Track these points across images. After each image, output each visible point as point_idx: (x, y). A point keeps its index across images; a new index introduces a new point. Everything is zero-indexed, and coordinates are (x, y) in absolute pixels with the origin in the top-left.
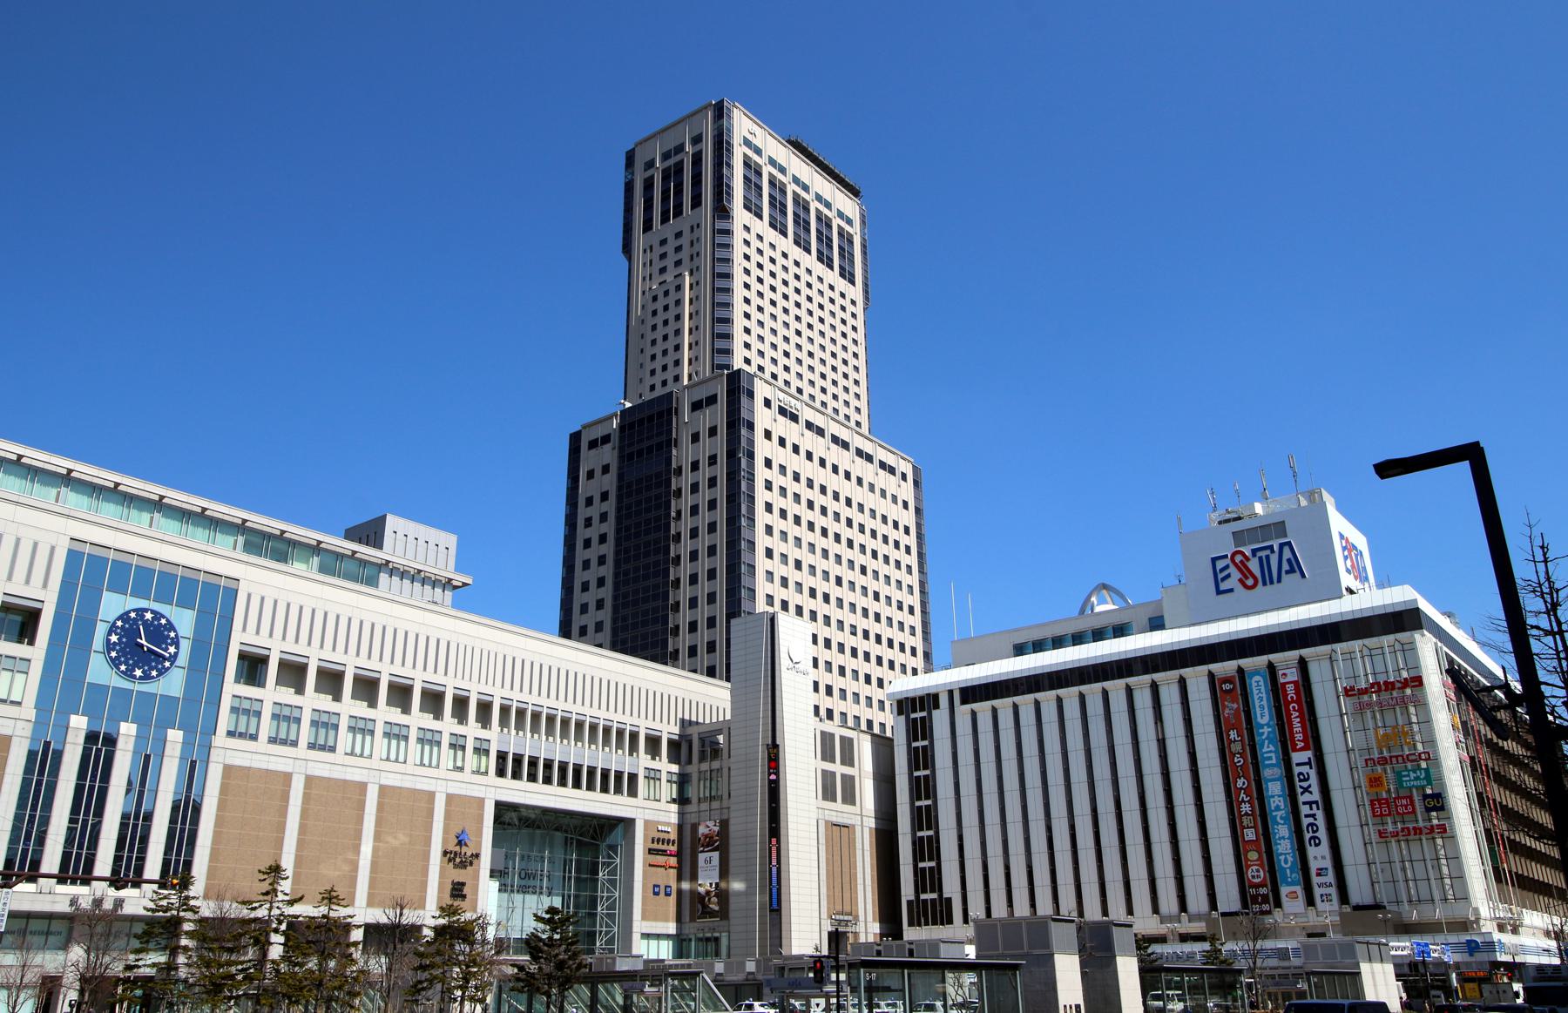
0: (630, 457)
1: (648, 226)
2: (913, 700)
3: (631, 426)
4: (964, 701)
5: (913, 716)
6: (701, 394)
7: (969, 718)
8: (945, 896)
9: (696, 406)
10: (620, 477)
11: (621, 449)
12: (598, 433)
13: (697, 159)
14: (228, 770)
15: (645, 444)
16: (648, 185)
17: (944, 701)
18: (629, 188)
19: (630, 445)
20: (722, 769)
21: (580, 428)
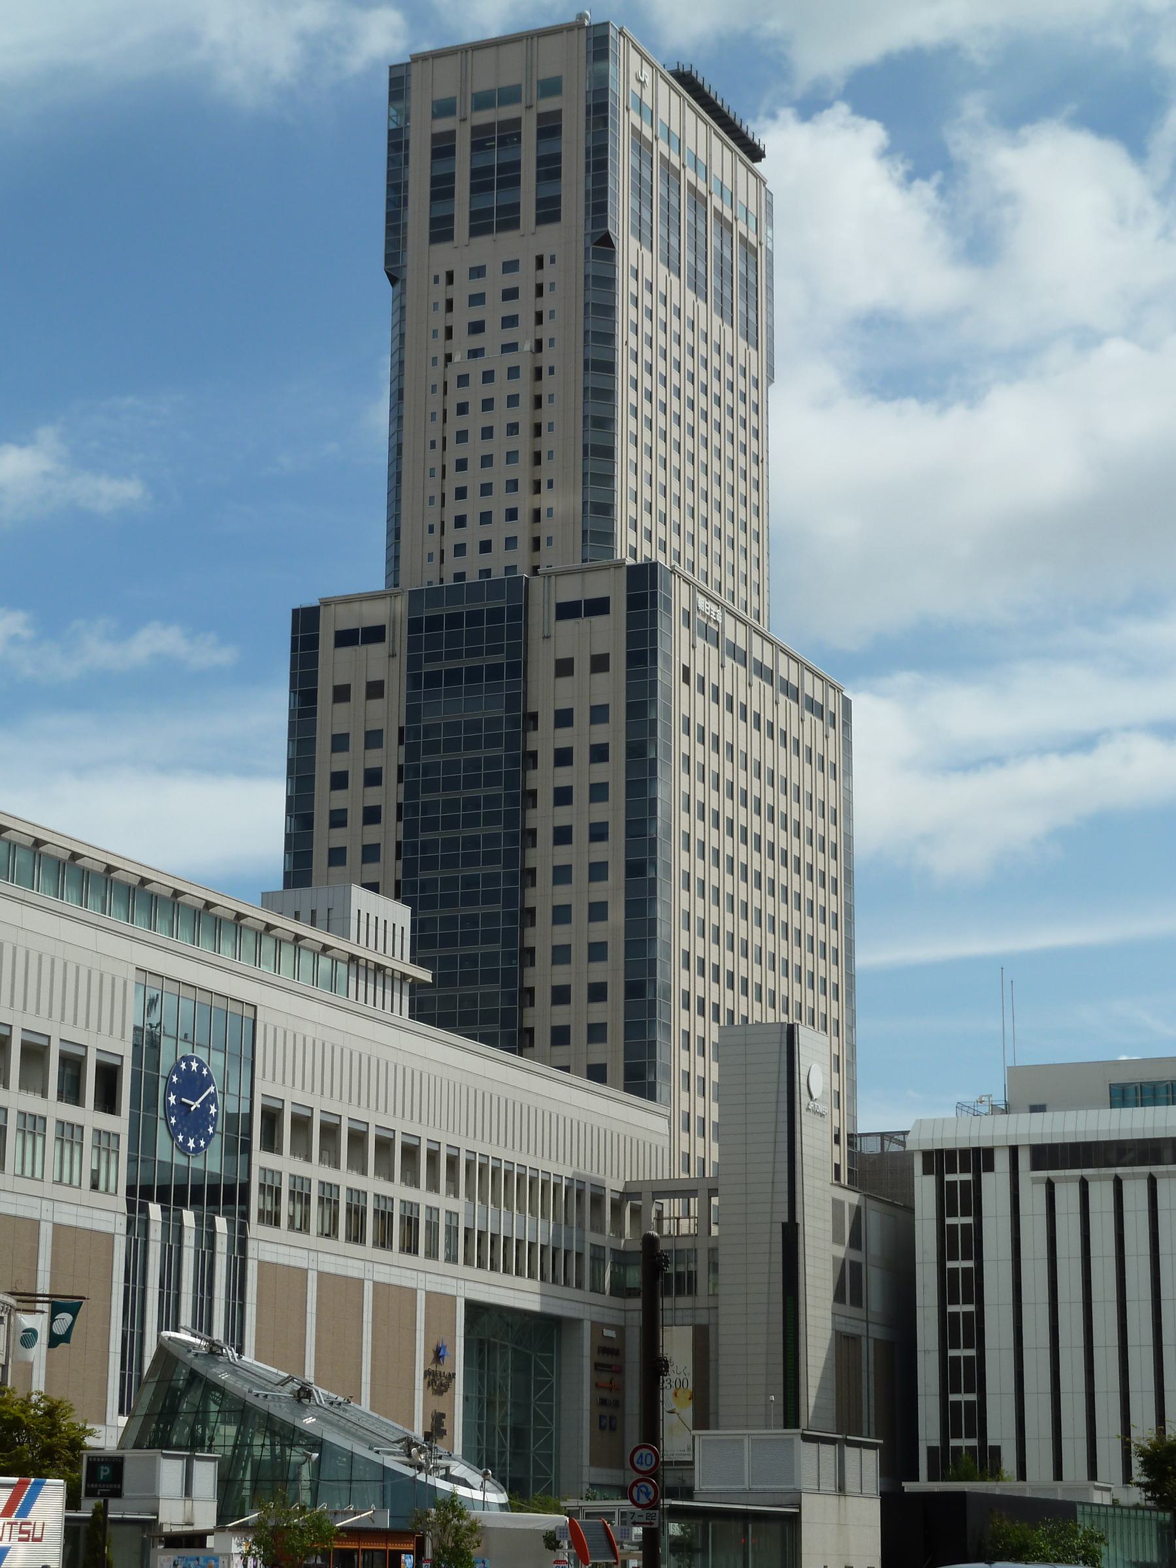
0: (433, 679)
1: (441, 230)
2: (951, 1153)
3: (434, 623)
4: (1036, 1166)
5: (949, 1178)
6: (570, 591)
7: (1041, 1190)
8: (990, 1443)
9: (567, 611)
10: (413, 713)
11: (413, 663)
12: (348, 619)
13: (550, 127)
14: (262, 1264)
15: (465, 663)
16: (443, 148)
17: (1002, 1161)
18: (397, 143)
19: (430, 658)
20: (696, 1250)
21: (318, 604)
